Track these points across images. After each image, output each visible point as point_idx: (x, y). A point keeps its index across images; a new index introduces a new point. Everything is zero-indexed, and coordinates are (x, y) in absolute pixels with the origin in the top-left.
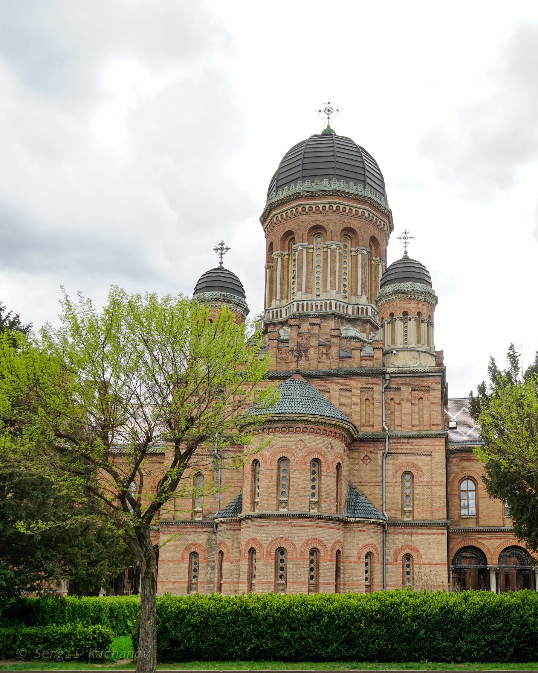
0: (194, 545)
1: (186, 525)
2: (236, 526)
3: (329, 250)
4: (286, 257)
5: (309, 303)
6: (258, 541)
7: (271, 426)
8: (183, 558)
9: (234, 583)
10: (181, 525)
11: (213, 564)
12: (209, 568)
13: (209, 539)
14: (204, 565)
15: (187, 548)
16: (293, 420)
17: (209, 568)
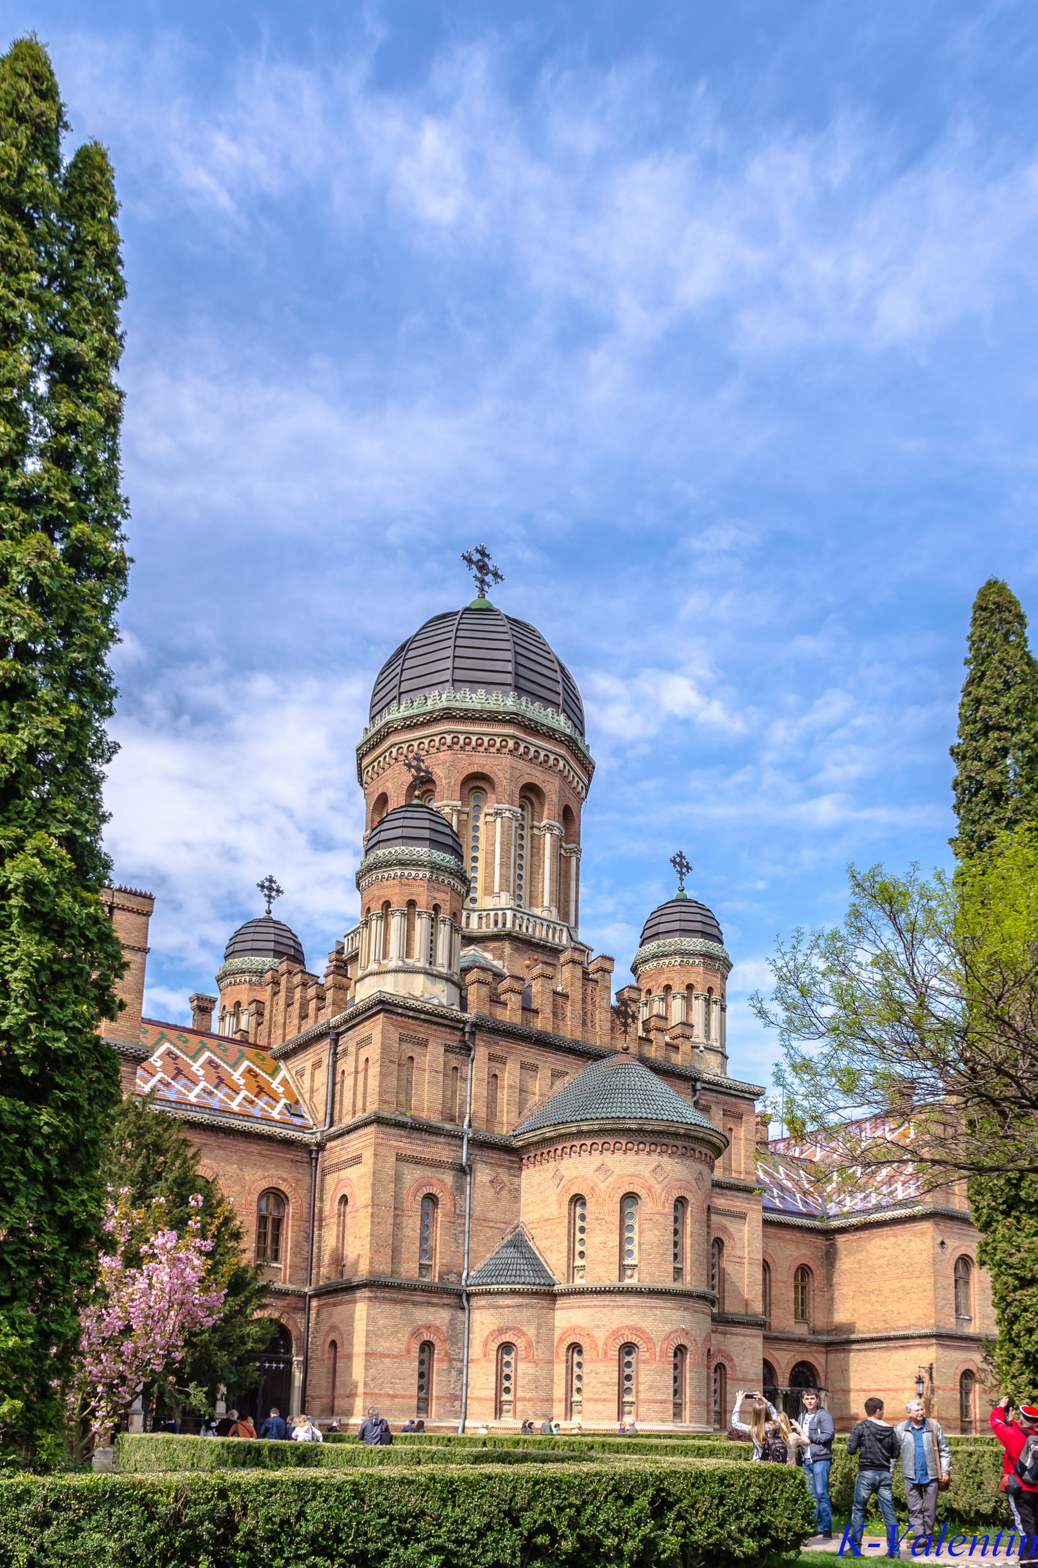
0: (428, 1328)
1: (415, 1290)
2: (544, 1303)
3: (548, 836)
4: (465, 817)
5: (532, 919)
6: (644, 1332)
7: (666, 1141)
8: (409, 1351)
9: (542, 1400)
10: (405, 1289)
11: (459, 1364)
12: (454, 1373)
13: (451, 1320)
14: (445, 1366)
15: (416, 1333)
16: (702, 1140)
17: (454, 1373)
